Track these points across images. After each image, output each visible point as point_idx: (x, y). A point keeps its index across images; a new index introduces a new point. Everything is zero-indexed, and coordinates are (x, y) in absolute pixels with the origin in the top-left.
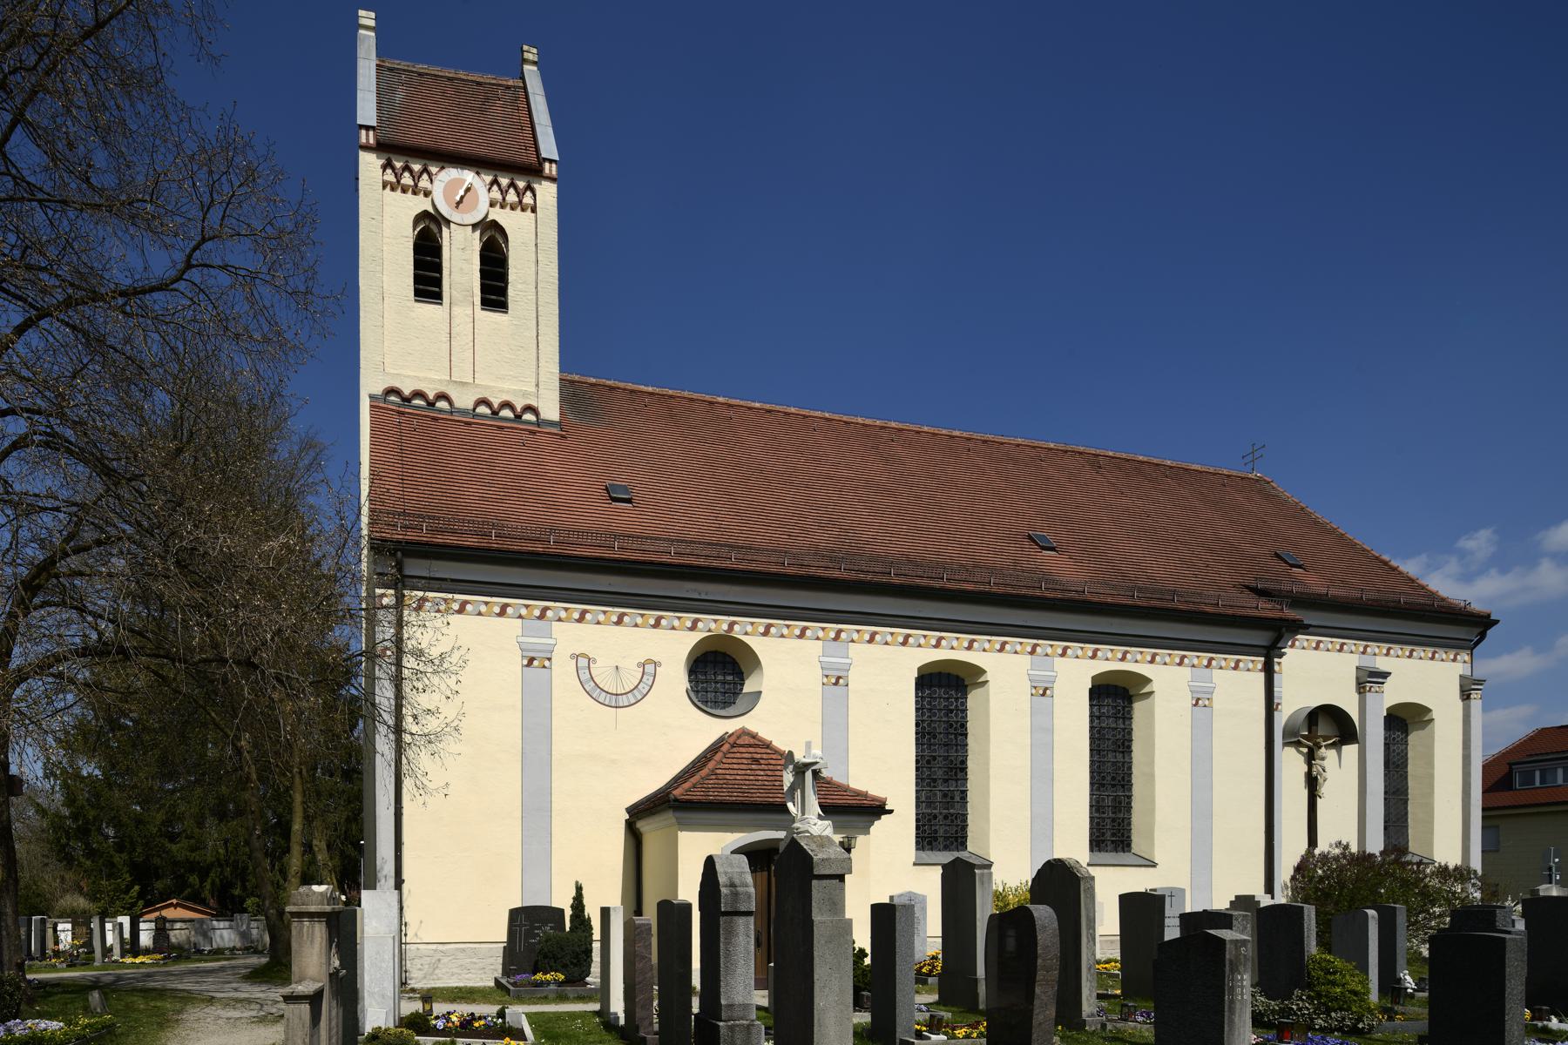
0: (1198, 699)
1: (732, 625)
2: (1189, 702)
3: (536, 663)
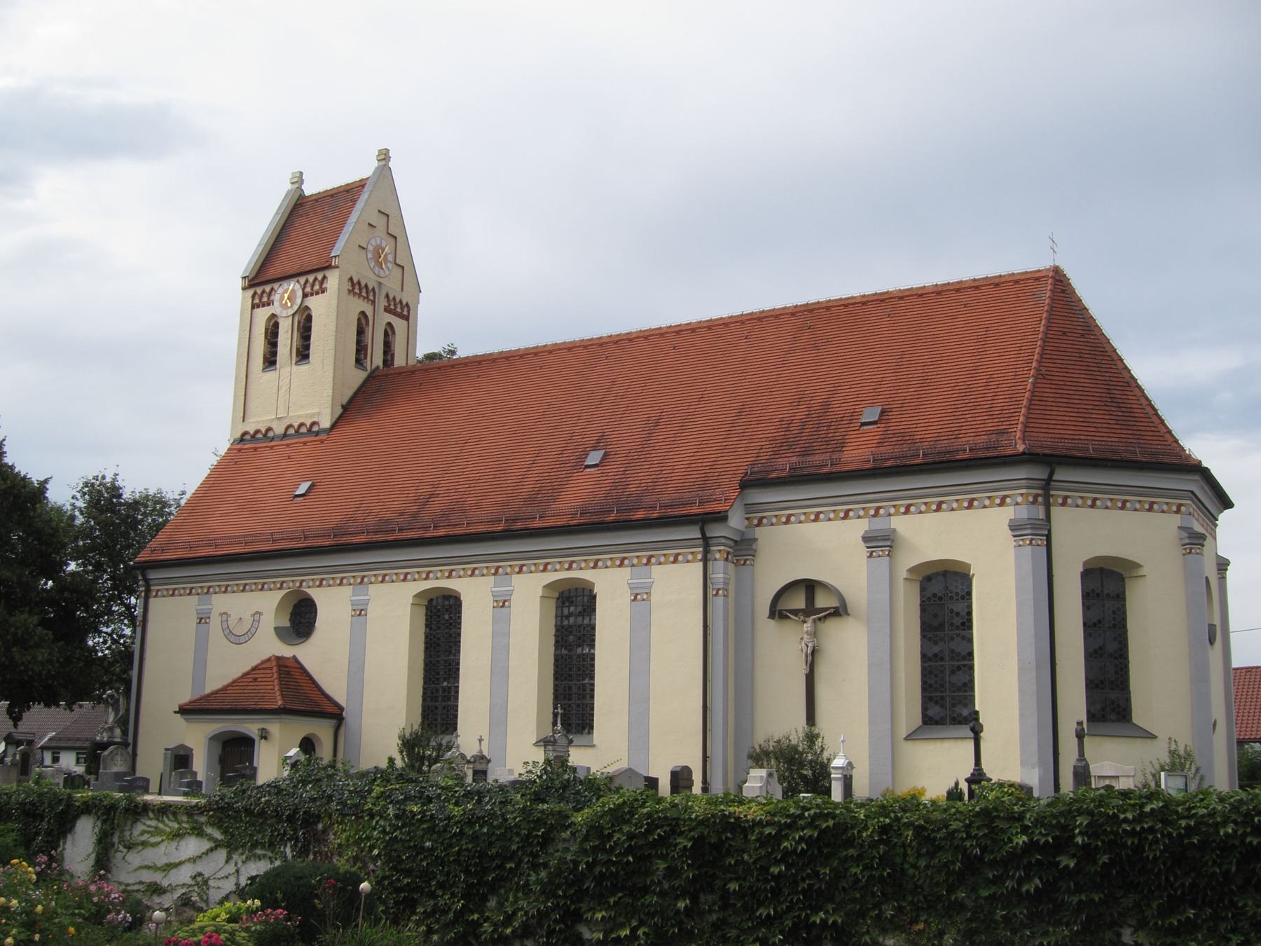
0: (636, 595)
1: (302, 582)
2: (628, 597)
3: (203, 621)
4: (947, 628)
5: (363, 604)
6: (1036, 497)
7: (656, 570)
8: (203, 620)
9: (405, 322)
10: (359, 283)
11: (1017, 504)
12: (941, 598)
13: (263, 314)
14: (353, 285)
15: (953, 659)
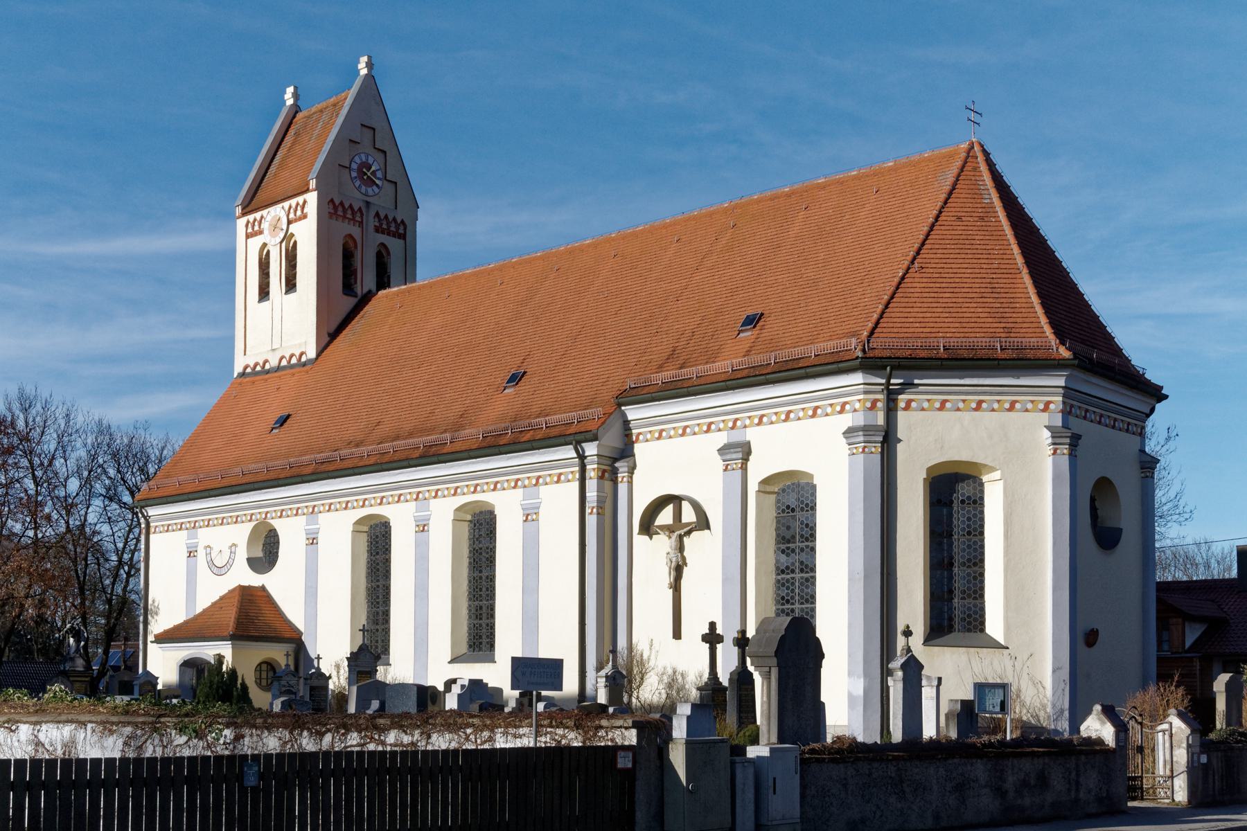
0: (528, 515)
3: (192, 554)
4: (797, 540)
5: (314, 533)
6: (874, 402)
7: (542, 489)
8: (191, 554)
9: (402, 241)
10: (342, 204)
11: (855, 410)
12: (793, 510)
13: (256, 243)
14: (335, 208)
15: (802, 570)
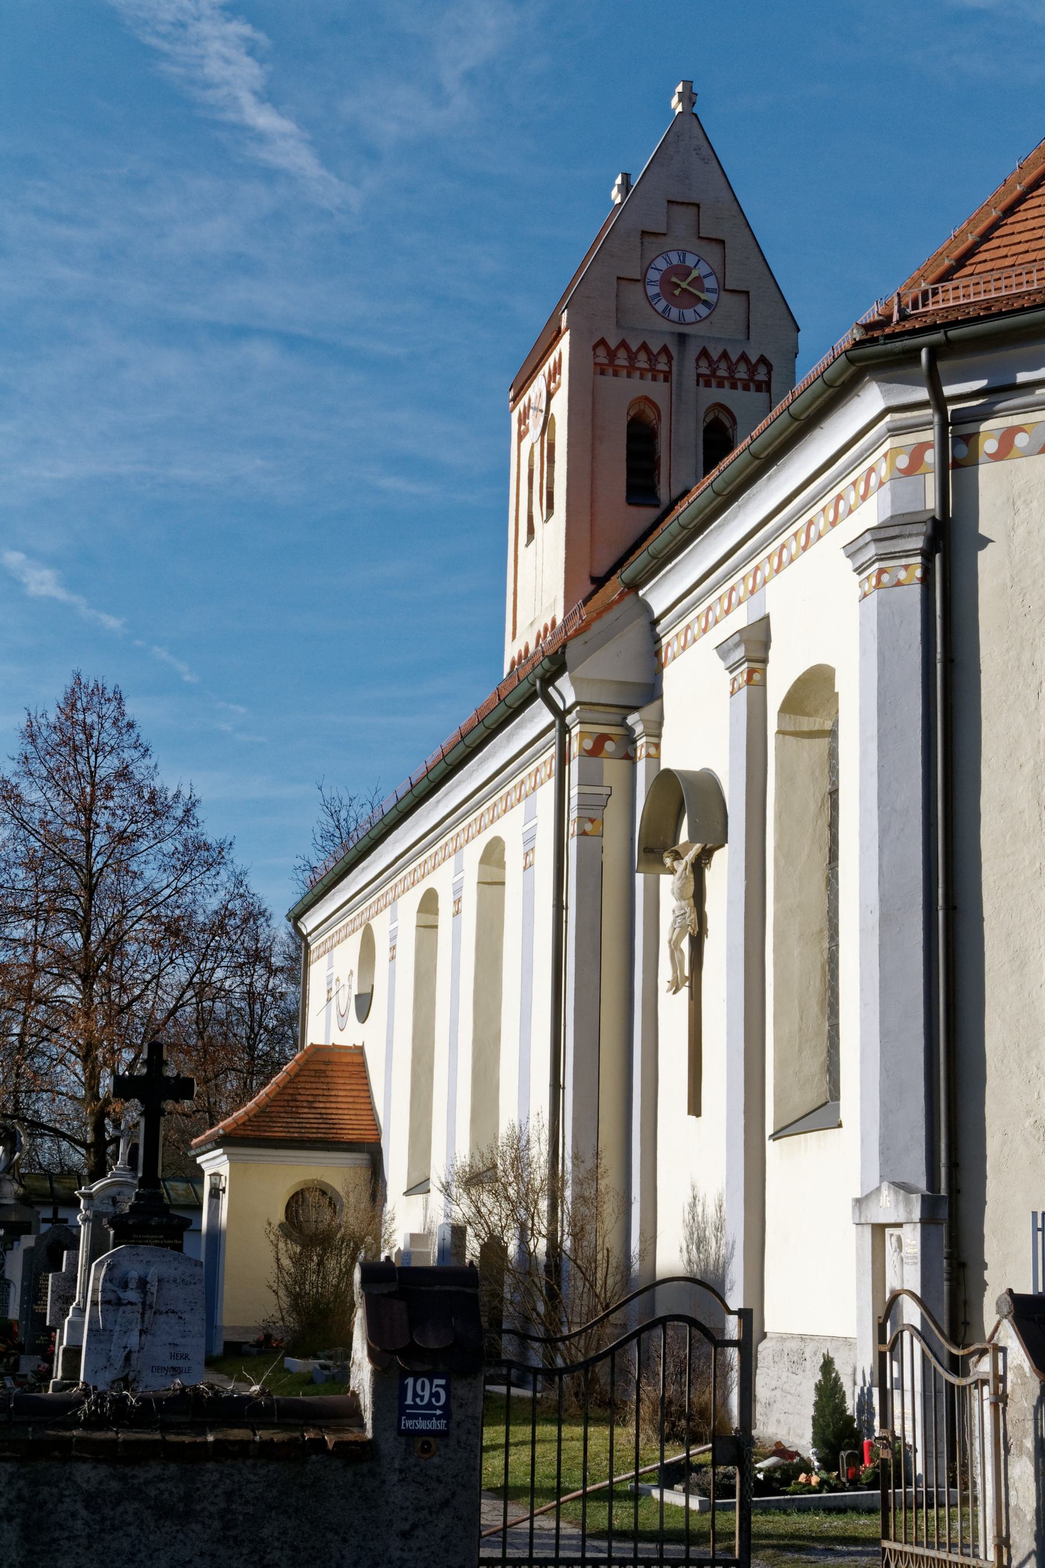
14: (612, 355)
